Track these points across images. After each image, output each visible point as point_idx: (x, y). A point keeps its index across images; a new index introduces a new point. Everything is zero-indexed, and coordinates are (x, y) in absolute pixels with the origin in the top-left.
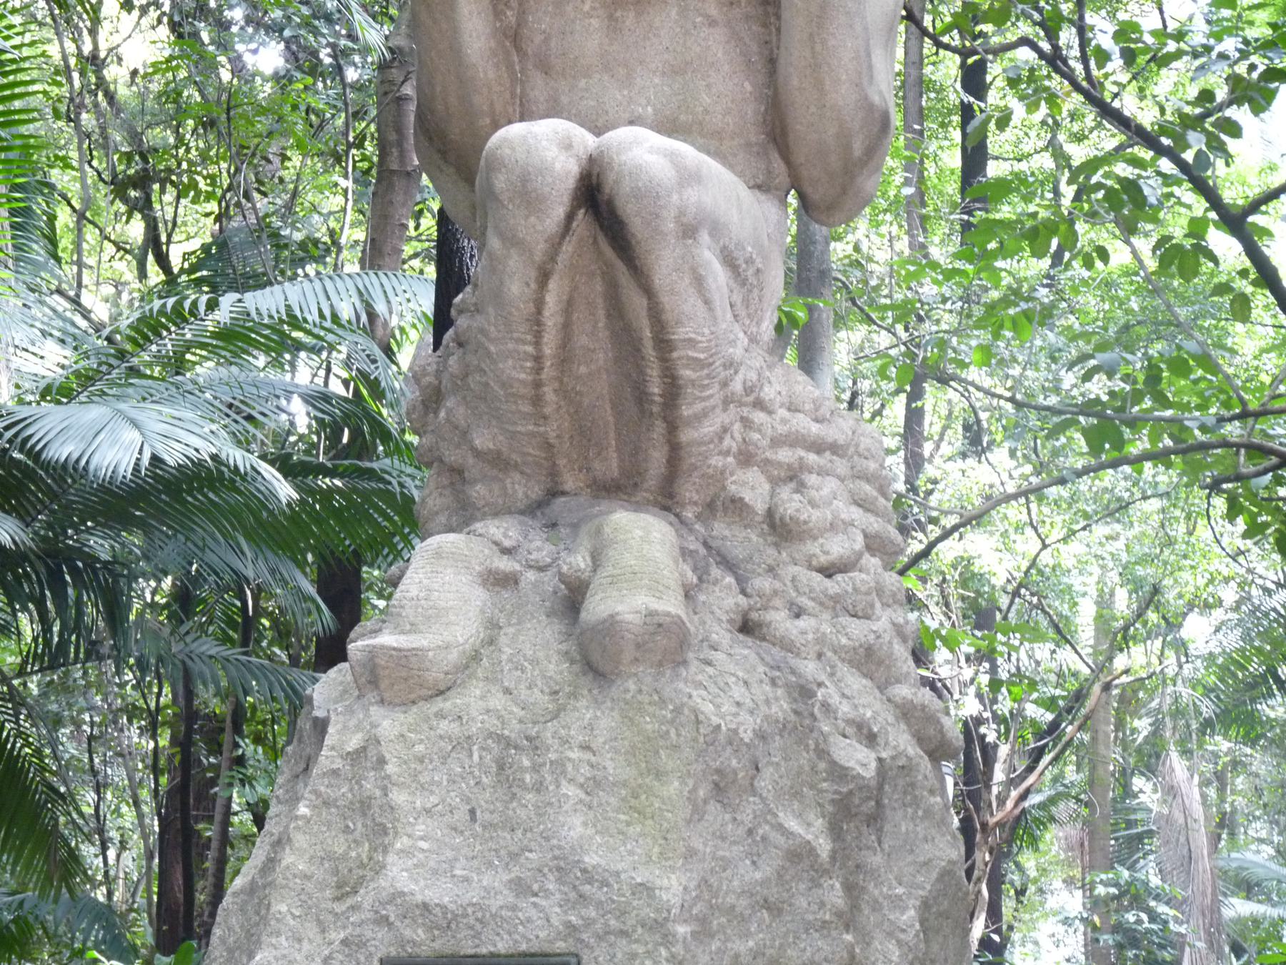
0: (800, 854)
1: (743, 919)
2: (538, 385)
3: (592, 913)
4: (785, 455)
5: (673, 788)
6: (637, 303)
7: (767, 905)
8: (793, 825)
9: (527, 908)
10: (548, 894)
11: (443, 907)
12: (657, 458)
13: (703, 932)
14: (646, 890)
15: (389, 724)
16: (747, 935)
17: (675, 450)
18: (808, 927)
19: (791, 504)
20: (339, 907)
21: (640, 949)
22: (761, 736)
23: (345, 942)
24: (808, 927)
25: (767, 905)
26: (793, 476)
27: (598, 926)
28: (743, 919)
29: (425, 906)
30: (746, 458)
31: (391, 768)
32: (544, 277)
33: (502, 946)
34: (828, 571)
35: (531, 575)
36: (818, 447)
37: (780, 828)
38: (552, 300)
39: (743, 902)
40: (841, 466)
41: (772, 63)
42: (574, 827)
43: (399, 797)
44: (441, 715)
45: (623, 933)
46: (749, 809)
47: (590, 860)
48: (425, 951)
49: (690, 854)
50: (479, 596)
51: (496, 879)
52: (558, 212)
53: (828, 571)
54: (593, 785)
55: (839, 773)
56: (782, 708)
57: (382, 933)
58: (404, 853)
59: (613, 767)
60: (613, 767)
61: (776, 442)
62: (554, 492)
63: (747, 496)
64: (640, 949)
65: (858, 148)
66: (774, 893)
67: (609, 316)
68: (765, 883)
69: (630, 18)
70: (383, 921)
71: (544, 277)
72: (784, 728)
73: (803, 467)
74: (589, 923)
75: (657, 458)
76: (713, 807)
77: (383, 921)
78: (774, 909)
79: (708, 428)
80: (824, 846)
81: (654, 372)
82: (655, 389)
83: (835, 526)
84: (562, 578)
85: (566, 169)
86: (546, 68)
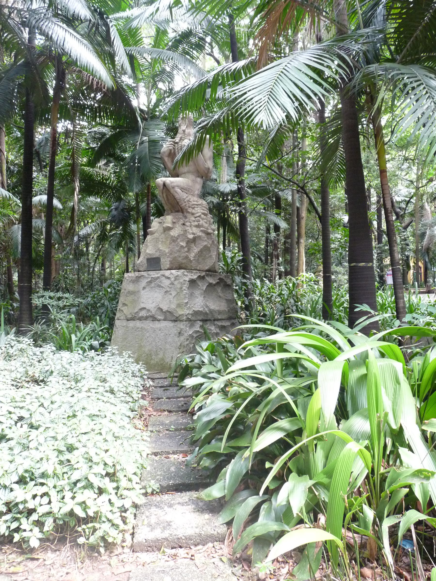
0: (182, 246)
5: (168, 242)
19: (194, 211)
22: (178, 236)
26: (193, 208)
30: (189, 207)
32: (163, 193)
33: (154, 257)
36: (197, 205)
38: (164, 195)
40: (200, 206)
41: (195, 165)
42: (160, 246)
50: (158, 224)
52: (162, 187)
54: (162, 242)
55: (188, 238)
56: (182, 233)
59: (164, 240)
60: (164, 240)
61: (192, 205)
65: (206, 172)
71: (163, 193)
72: (182, 235)
73: (195, 207)
78: (180, 251)
79: (183, 205)
85: (162, 183)
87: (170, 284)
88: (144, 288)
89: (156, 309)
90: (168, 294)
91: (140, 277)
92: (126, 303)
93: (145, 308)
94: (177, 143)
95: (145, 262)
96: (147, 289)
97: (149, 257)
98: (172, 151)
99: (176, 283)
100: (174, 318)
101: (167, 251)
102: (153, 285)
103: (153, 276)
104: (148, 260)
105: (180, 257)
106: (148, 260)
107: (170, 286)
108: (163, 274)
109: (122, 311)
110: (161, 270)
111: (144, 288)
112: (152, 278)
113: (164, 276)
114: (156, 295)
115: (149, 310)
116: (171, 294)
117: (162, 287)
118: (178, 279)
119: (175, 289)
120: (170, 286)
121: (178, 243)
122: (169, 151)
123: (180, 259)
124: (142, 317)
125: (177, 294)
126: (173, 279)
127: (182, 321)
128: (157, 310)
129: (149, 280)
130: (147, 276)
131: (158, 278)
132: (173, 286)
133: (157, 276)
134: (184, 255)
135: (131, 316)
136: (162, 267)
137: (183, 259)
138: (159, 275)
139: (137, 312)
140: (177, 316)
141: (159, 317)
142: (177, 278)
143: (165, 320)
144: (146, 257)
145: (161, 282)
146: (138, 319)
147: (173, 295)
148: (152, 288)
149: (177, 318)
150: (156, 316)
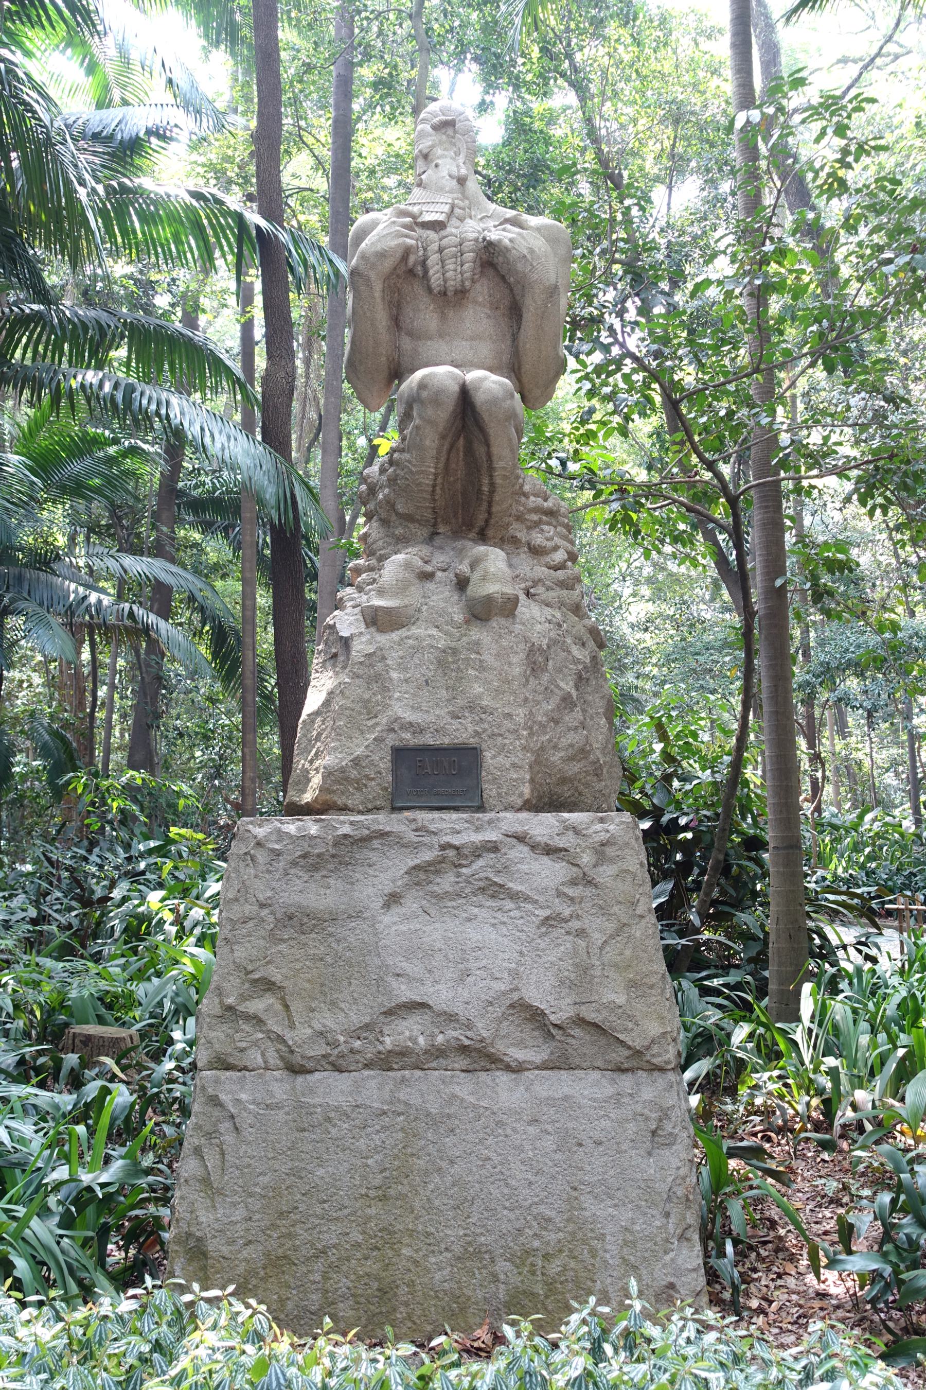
1: (545, 727)
2: (434, 486)
3: (486, 726)
4: (535, 517)
6: (480, 450)
7: (553, 720)
8: (562, 685)
9: (456, 724)
10: (465, 718)
11: (419, 724)
12: (482, 516)
13: (531, 734)
14: (509, 716)
15: (383, 639)
16: (546, 733)
17: (490, 513)
18: (569, 729)
19: (538, 539)
20: (370, 723)
21: (507, 741)
23: (375, 739)
24: (569, 729)
25: (553, 720)
27: (489, 732)
28: (545, 727)
29: (411, 724)
31: (389, 662)
33: (447, 740)
34: (556, 568)
35: (439, 574)
37: (558, 686)
39: (544, 719)
43: (394, 675)
44: (408, 637)
45: (501, 735)
46: (546, 678)
47: (485, 703)
48: (412, 743)
49: (526, 700)
51: (443, 712)
53: (556, 568)
57: (392, 735)
58: (398, 699)
62: (435, 534)
63: (519, 535)
64: (507, 741)
66: (556, 715)
67: (465, 455)
68: (553, 710)
69: (451, 314)
70: (393, 730)
74: (485, 730)
75: (482, 517)
76: (531, 679)
77: (392, 730)
78: (557, 722)
80: (574, 693)
81: (486, 481)
82: (485, 489)
83: (556, 548)
84: (456, 575)
86: (410, 334)
87: (573, 883)
88: (393, 899)
89: (498, 1011)
90: (555, 933)
91: (365, 840)
92: (277, 978)
93: (423, 1005)
94: (437, 226)
95: (385, 765)
96: (412, 903)
97: (408, 738)
98: (412, 259)
99: (606, 874)
100: (619, 1055)
101: (520, 714)
102: (446, 882)
103: (456, 841)
104: (400, 754)
105: (555, 747)
106: (400, 754)
107: (570, 891)
108: (518, 829)
109: (257, 1021)
110: (481, 808)
111: (393, 899)
112: (443, 847)
113: (521, 838)
114: (475, 934)
115: (451, 1018)
116: (581, 933)
117: (514, 896)
118: (612, 860)
119: (604, 911)
120: (570, 891)
121: (552, 681)
122: (399, 255)
123: (556, 757)
124: (403, 1053)
125: (618, 932)
126: (586, 859)
127: (662, 1070)
128: (505, 1017)
129: (427, 856)
130: (411, 836)
131: (493, 848)
132: (589, 892)
133: (477, 838)
134: (571, 738)
135: (320, 1049)
136: (490, 790)
137: (571, 759)
138: (492, 836)
139: (367, 1027)
140: (638, 1044)
141: (518, 1054)
142: (610, 851)
143: (544, 1066)
144: (391, 740)
145: (506, 869)
146: (367, 1066)
147: (598, 938)
148: (439, 897)
149: (638, 1053)
150: (500, 1047)
